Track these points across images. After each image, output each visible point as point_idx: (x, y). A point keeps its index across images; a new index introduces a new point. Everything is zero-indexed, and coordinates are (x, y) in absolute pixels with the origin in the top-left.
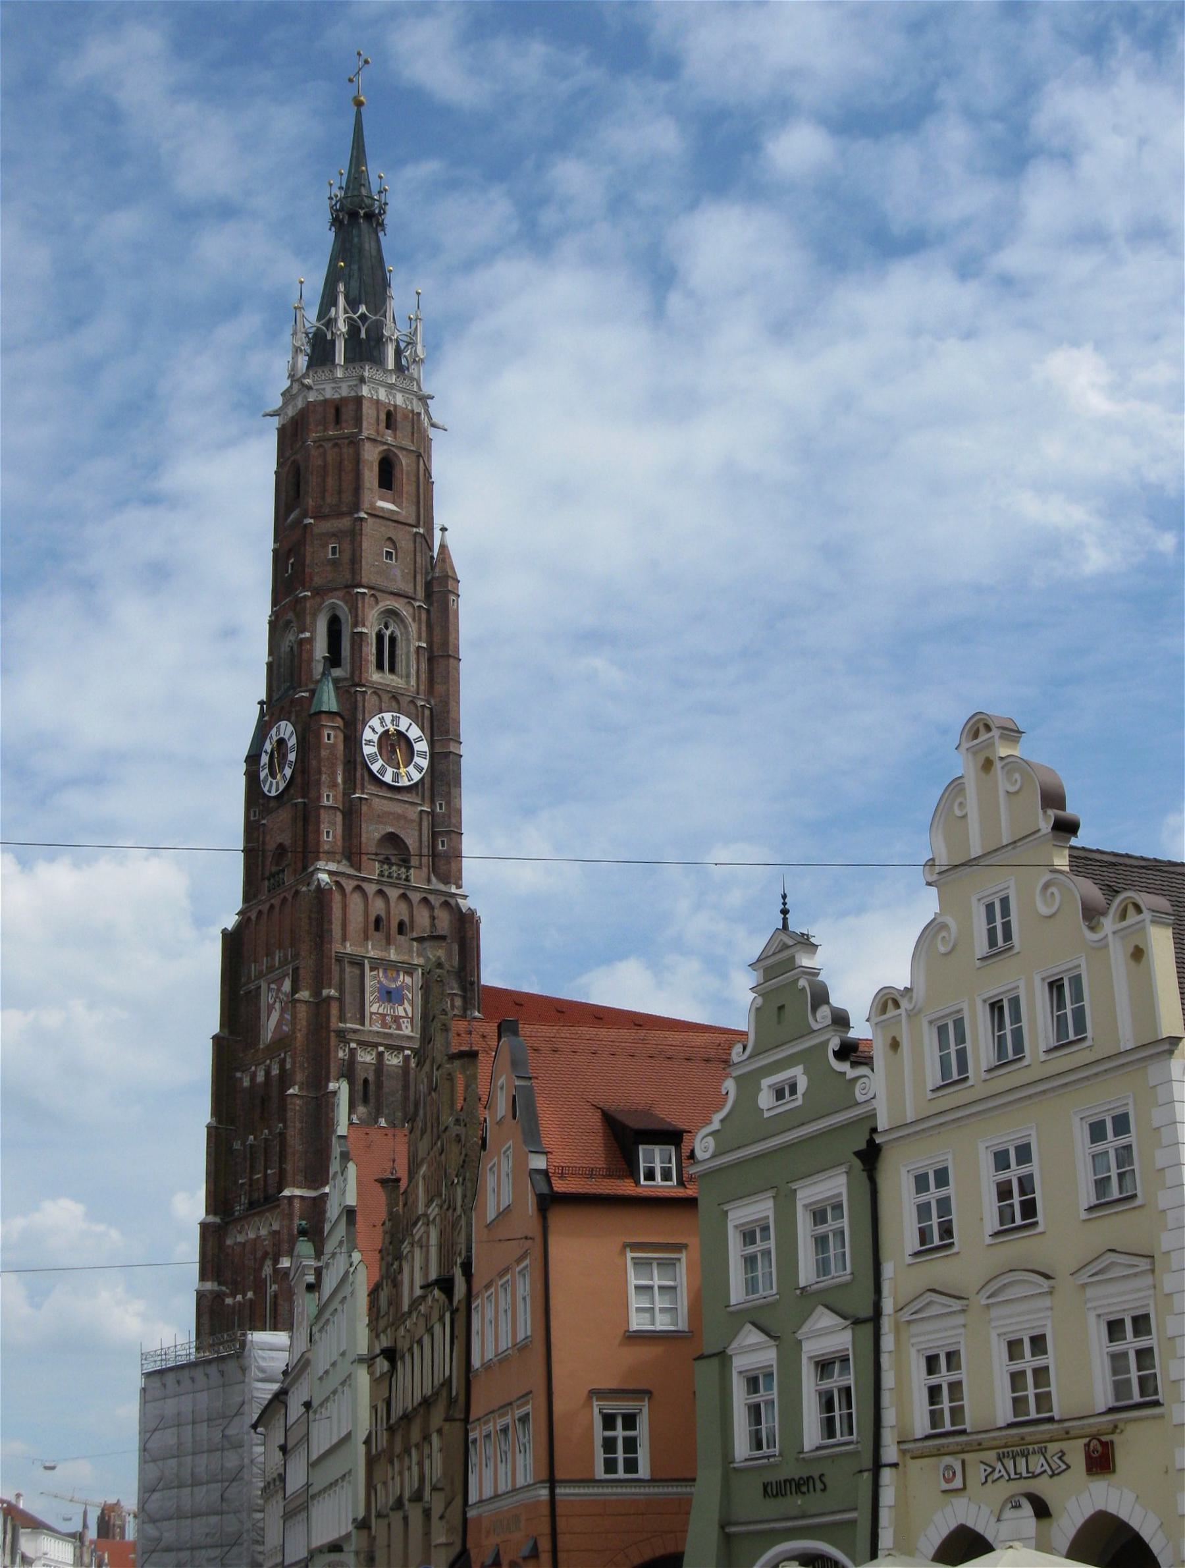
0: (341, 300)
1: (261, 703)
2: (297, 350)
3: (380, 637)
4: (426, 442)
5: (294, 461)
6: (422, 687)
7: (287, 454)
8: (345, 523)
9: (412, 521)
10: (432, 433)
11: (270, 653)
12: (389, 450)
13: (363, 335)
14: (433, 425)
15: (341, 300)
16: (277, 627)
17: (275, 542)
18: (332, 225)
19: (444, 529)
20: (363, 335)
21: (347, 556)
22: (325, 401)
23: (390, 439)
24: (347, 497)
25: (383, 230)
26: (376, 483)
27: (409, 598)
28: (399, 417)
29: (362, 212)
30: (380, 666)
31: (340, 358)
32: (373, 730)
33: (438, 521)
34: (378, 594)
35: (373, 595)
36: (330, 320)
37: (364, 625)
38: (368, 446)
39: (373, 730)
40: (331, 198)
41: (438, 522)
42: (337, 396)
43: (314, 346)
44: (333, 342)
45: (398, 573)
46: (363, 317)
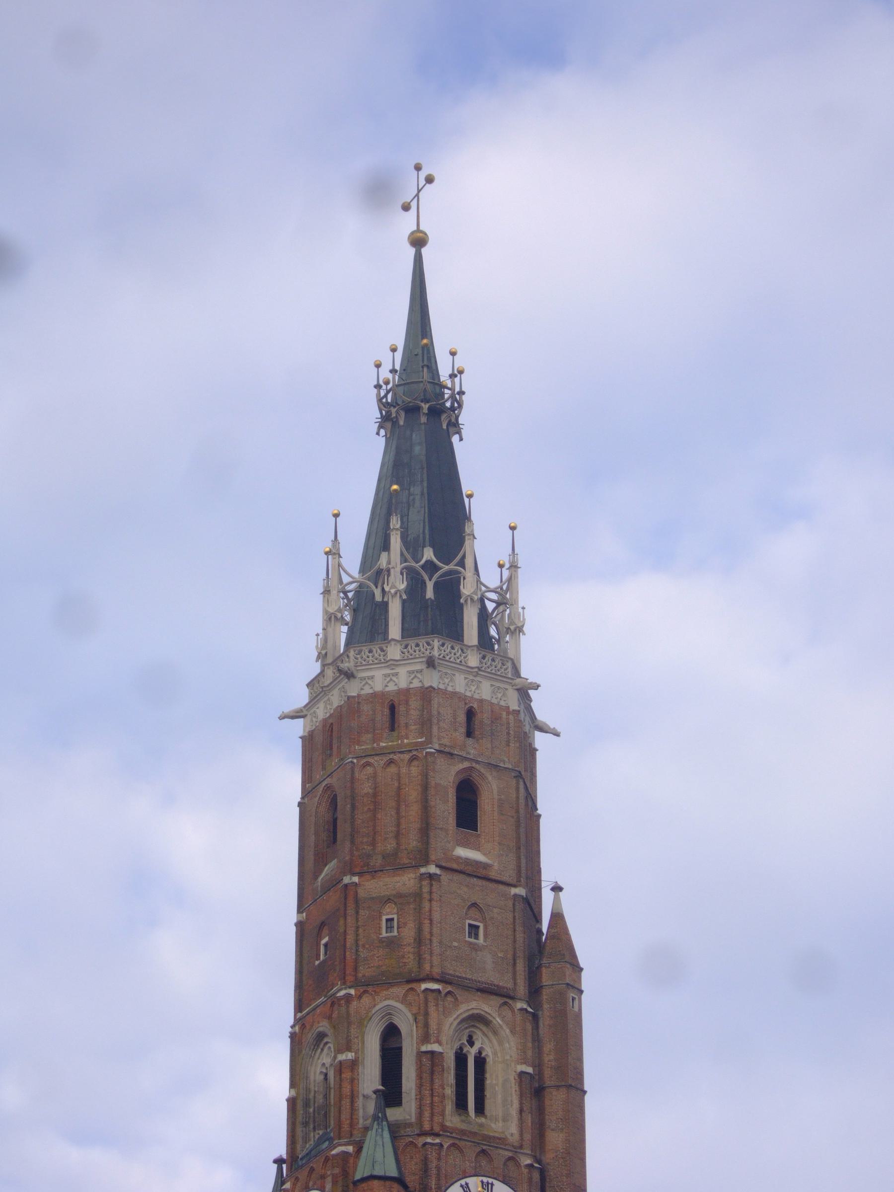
0: (396, 542)
1: (279, 1161)
2: (331, 618)
3: (461, 1059)
4: (529, 754)
5: (328, 788)
6: (528, 1137)
7: (317, 777)
8: (406, 881)
9: (505, 878)
10: (540, 740)
11: (293, 1085)
13: (430, 594)
14: (542, 728)
15: (396, 542)
16: (302, 1044)
17: (300, 911)
18: (381, 427)
19: (557, 889)
20: (430, 594)
21: (409, 933)
22: (375, 695)
23: (473, 753)
24: (412, 841)
25: (459, 432)
26: (452, 820)
27: (505, 996)
28: (484, 717)
29: (425, 407)
30: (461, 1103)
31: (395, 630)
33: (549, 874)
34: (458, 992)
35: (449, 993)
36: (379, 572)
37: (439, 1042)
38: (441, 762)
40: (378, 387)
41: (547, 877)
42: (391, 687)
43: (355, 611)
44: (384, 606)
45: (489, 959)
46: (431, 567)
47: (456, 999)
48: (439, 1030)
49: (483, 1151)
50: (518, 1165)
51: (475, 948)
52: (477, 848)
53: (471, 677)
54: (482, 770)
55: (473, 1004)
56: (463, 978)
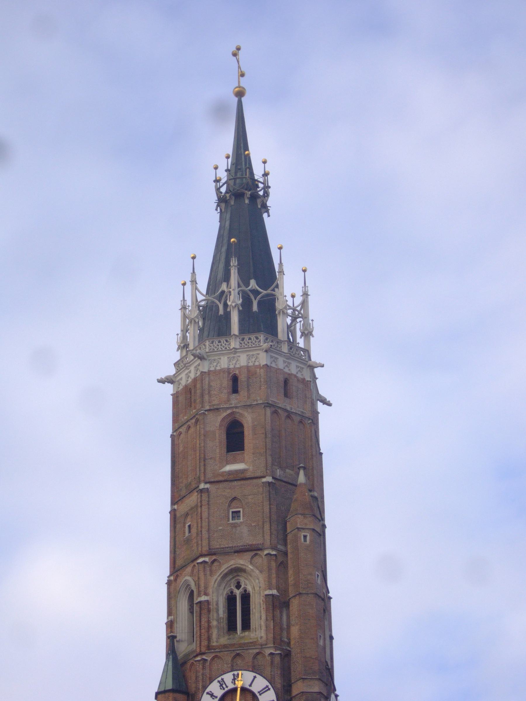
3: (231, 599)
9: (258, 474)
12: (233, 413)
27: (254, 550)
28: (242, 378)
30: (232, 627)
32: (212, 695)
35: (215, 560)
37: (206, 594)
38: (211, 417)
39: (212, 695)
45: (245, 530)
47: (220, 562)
48: (206, 588)
49: (238, 655)
50: (264, 656)
51: (234, 526)
52: (242, 461)
53: (232, 355)
54: (241, 411)
55: (232, 562)
56: (226, 548)
